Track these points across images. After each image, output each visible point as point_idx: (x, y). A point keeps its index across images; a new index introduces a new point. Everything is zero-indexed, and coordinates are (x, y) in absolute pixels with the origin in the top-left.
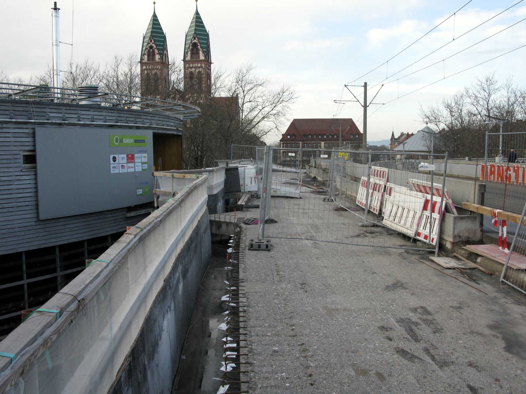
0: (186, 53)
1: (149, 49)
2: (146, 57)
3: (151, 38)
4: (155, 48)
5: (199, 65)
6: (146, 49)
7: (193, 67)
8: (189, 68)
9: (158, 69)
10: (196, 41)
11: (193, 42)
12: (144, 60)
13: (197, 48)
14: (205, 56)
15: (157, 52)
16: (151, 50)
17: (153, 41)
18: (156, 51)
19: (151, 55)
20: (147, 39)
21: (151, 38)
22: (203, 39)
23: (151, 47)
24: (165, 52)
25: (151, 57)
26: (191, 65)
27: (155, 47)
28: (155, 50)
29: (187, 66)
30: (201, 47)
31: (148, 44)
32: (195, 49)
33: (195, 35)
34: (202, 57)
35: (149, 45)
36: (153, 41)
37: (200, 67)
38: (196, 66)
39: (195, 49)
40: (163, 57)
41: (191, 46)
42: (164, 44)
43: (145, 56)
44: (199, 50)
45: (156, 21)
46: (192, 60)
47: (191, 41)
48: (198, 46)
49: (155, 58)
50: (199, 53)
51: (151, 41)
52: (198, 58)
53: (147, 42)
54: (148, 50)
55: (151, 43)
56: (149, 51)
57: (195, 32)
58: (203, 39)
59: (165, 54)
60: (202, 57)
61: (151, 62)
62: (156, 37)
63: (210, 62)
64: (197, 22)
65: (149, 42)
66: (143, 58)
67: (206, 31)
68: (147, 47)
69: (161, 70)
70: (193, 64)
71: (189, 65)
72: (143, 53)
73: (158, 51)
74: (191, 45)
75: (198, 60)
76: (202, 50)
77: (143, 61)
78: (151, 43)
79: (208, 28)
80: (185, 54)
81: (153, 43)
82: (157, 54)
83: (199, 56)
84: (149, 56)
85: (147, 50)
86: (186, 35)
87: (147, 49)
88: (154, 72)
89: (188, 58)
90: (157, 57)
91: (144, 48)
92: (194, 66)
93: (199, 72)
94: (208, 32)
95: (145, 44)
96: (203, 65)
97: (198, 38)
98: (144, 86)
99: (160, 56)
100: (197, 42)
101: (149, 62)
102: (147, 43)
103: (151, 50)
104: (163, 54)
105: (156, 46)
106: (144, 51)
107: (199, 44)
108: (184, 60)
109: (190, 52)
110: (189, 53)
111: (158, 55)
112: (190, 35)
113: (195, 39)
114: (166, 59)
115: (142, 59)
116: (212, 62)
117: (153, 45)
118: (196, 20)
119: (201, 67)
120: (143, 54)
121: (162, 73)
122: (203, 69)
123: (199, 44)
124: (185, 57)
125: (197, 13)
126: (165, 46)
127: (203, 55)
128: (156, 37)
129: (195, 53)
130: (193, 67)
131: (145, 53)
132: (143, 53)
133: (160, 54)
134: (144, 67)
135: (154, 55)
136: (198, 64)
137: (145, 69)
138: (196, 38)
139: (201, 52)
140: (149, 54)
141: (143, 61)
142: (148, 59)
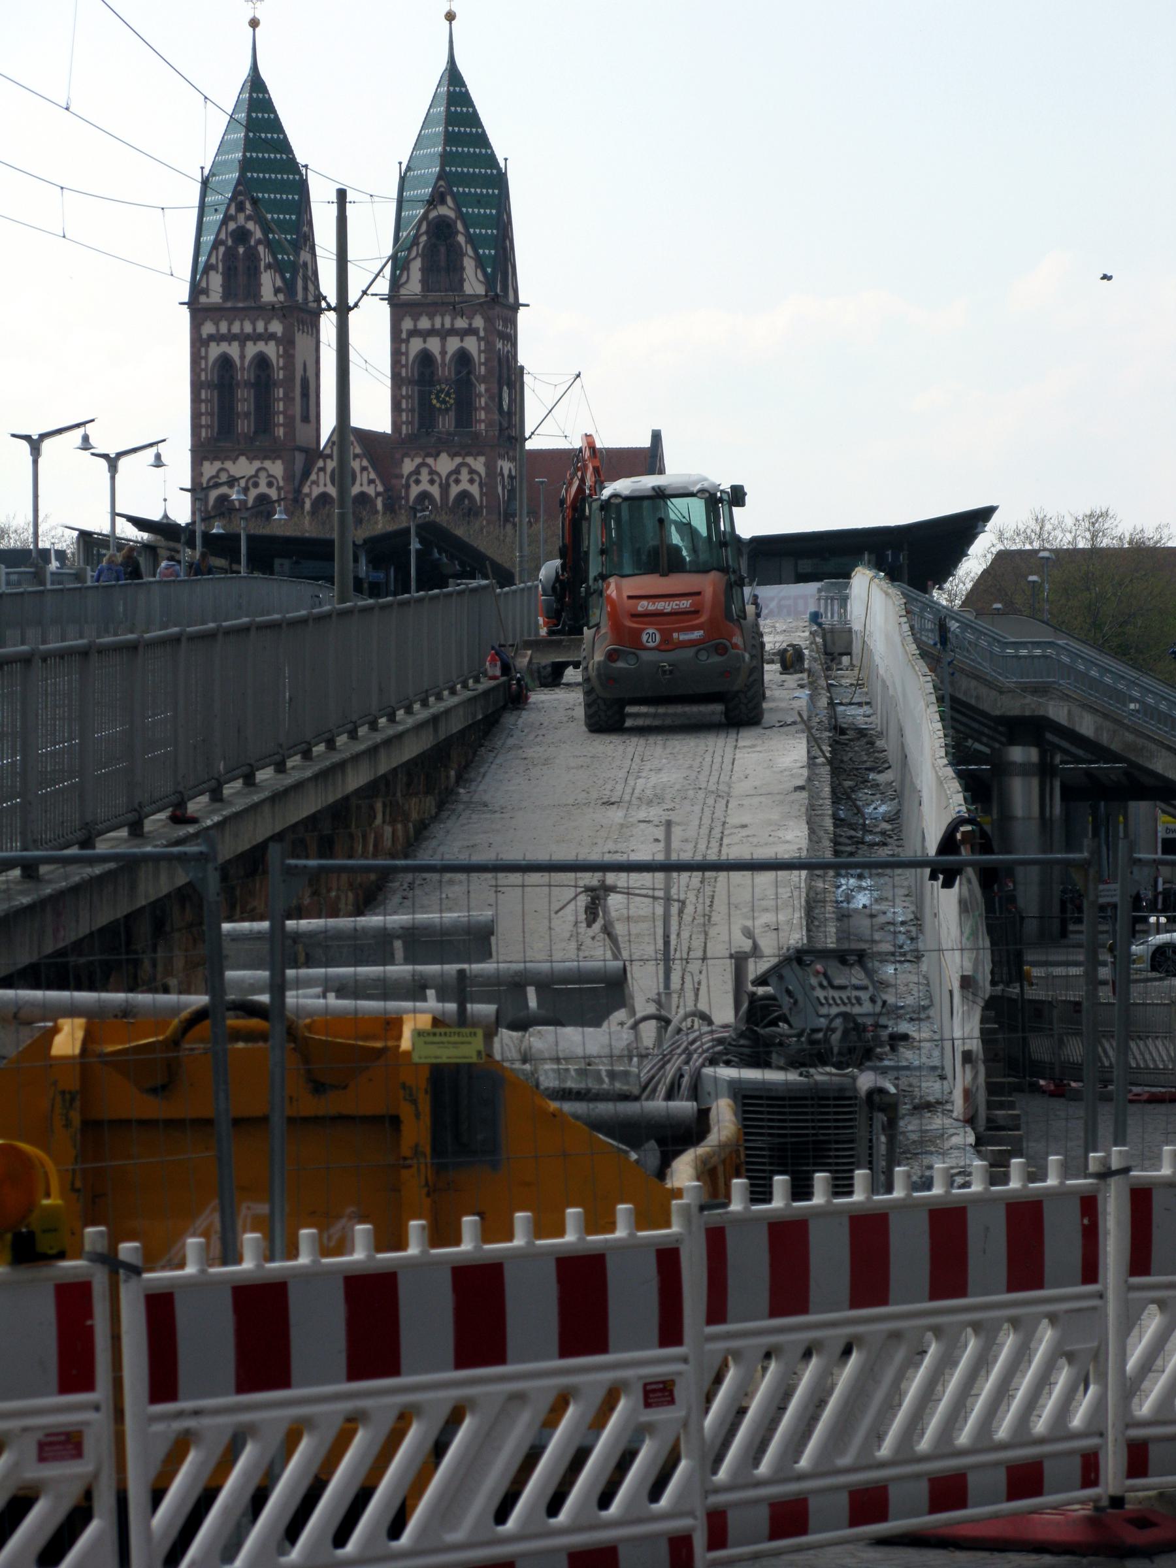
0: (400, 263)
1: (230, 242)
2: (216, 281)
3: (240, 193)
4: (259, 242)
5: (461, 323)
6: (216, 244)
7: (431, 332)
8: (414, 333)
9: (272, 337)
10: (446, 211)
12: (206, 292)
14: (489, 282)
16: (241, 250)
19: (241, 267)
20: (220, 197)
21: (240, 193)
22: (479, 201)
23: (241, 235)
24: (304, 256)
26: (424, 323)
27: (258, 234)
28: (261, 248)
29: (407, 324)
30: (470, 239)
31: (225, 222)
33: (441, 183)
35: (232, 226)
37: (463, 333)
38: (448, 325)
39: (443, 249)
41: (427, 232)
42: (298, 218)
43: (212, 274)
44: (461, 254)
48: (457, 232)
49: (260, 285)
50: (463, 269)
53: (223, 208)
54: (228, 249)
55: (241, 217)
56: (230, 254)
58: (479, 201)
59: (305, 264)
60: (473, 284)
61: (240, 305)
62: (264, 185)
63: (511, 299)
64: (450, 139)
65: (232, 211)
66: (204, 284)
67: (491, 160)
68: (223, 236)
69: (287, 342)
70: (431, 317)
71: (416, 319)
72: (203, 259)
74: (424, 228)
77: (203, 299)
81: (248, 218)
82: (269, 266)
84: (229, 275)
85: (222, 249)
86: (403, 180)
87: (222, 243)
88: (252, 350)
90: (268, 286)
91: (208, 239)
92: (438, 325)
93: (463, 357)
94: (502, 165)
96: (479, 322)
98: (207, 413)
99: (283, 278)
100: (452, 214)
101: (229, 305)
102: (220, 217)
103: (241, 250)
106: (205, 250)
107: (460, 227)
108: (393, 298)
109: (419, 260)
110: (416, 265)
112: (420, 182)
113: (443, 201)
114: (306, 289)
115: (197, 290)
116: (521, 301)
117: (250, 225)
118: (446, 128)
119: (471, 331)
121: (289, 356)
122: (479, 339)
123: (460, 227)
126: (305, 229)
128: (264, 185)
129: (443, 264)
130: (431, 332)
131: (213, 260)
133: (278, 267)
134: (208, 329)
135: (253, 273)
137: (211, 338)
138: (449, 200)
139: (469, 264)
140: (229, 269)
141: (203, 299)
142: (228, 293)
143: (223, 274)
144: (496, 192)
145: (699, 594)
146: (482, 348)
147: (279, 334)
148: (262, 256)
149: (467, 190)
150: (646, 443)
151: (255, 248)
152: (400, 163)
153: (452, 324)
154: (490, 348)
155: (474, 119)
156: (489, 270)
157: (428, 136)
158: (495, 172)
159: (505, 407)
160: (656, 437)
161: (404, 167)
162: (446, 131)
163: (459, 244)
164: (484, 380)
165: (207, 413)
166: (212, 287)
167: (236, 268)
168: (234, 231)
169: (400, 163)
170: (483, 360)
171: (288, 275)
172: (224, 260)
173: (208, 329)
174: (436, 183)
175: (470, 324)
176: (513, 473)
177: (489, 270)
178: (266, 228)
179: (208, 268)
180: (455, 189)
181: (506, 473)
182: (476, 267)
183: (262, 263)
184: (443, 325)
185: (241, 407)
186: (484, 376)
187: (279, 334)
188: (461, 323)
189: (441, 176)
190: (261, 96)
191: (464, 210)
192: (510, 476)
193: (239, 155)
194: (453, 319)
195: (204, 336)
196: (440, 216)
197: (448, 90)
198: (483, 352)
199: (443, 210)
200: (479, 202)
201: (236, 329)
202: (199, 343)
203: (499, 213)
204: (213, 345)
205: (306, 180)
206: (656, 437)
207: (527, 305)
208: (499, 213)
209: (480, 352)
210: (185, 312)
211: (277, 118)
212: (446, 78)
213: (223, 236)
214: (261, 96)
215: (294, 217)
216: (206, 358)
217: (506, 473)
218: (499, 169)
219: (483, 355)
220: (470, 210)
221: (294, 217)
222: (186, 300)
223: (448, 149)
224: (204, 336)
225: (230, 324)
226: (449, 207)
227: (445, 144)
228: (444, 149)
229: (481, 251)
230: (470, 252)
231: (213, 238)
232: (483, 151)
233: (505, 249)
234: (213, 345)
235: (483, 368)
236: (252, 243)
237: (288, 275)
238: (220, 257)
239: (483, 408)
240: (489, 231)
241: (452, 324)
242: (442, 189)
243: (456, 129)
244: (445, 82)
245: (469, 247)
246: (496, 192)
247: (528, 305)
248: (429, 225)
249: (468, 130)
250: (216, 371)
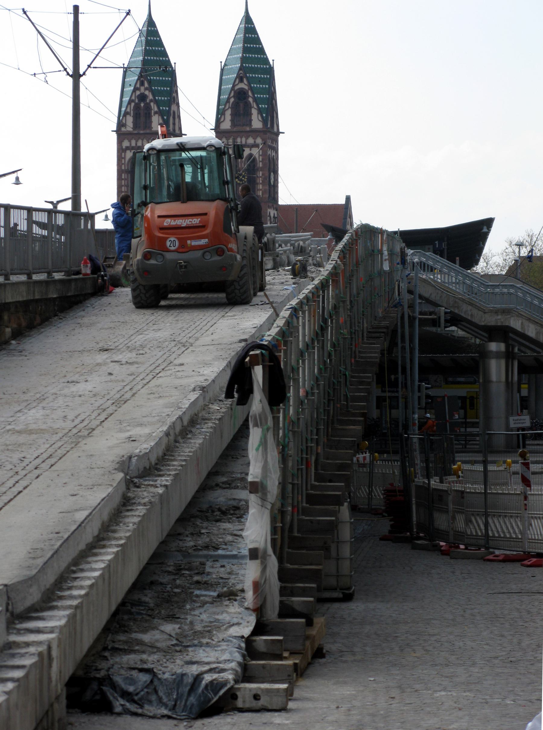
0: (221, 112)
1: (137, 101)
2: (130, 120)
4: (151, 101)
5: (251, 141)
6: (130, 103)
10: (243, 86)
11: (236, 88)
12: (124, 125)
13: (246, 103)
14: (265, 121)
15: (156, 109)
16: (142, 105)
17: (146, 85)
20: (133, 78)
22: (260, 81)
23: (143, 97)
24: (174, 107)
25: (142, 119)
27: (151, 97)
28: (152, 104)
30: (255, 100)
31: (134, 91)
32: (242, 105)
33: (241, 72)
34: (257, 123)
35: (138, 93)
36: (146, 85)
39: (242, 105)
41: (234, 96)
43: (128, 117)
44: (251, 107)
45: (154, 37)
46: (235, 129)
47: (234, 86)
48: (249, 96)
49: (151, 122)
50: (251, 114)
51: (142, 84)
52: (247, 125)
53: (133, 85)
55: (142, 89)
56: (137, 107)
57: (242, 65)
58: (260, 81)
59: (174, 112)
60: (257, 123)
61: (142, 132)
63: (275, 130)
64: (245, 50)
65: (138, 86)
67: (266, 61)
68: (133, 98)
72: (123, 109)
73: (159, 108)
74: (232, 94)
75: (248, 129)
76: (258, 106)
78: (142, 89)
79: (271, 53)
80: (220, 113)
81: (146, 89)
82: (156, 113)
83: (251, 120)
84: (136, 117)
85: (133, 104)
86: (222, 70)
89: (226, 125)
91: (126, 99)
94: (271, 63)
95: (129, 89)
96: (259, 141)
97: (247, 78)
98: (125, 186)
102: (132, 88)
103: (142, 105)
105: (154, 96)
106: (125, 104)
107: (250, 94)
109: (230, 110)
110: (228, 113)
111: (157, 116)
112: (231, 71)
113: (241, 81)
114: (174, 124)
115: (120, 124)
116: (280, 131)
117: (147, 93)
118: (244, 45)
119: (256, 146)
120: (122, 113)
123: (250, 94)
124: (218, 122)
125: (248, 19)
126: (174, 95)
127: (260, 118)
129: (242, 112)
132: (123, 109)
133: (161, 113)
134: (126, 144)
135: (148, 116)
136: (247, 138)
137: (127, 148)
138: (245, 81)
139: (254, 112)
140: (136, 114)
141: (123, 129)
143: (133, 117)
144: (268, 76)
145: (206, 214)
146: (261, 153)
148: (153, 108)
149: (254, 75)
150: (343, 202)
151: (149, 104)
152: (221, 62)
153: (246, 142)
154: (264, 154)
155: (258, 41)
156: (264, 115)
157: (235, 49)
158: (268, 66)
159: (272, 183)
160: (348, 199)
161: (223, 64)
162: (244, 46)
163: (249, 102)
164: (262, 169)
165: (125, 186)
166: (127, 124)
167: (140, 114)
168: (139, 95)
169: (221, 62)
170: (261, 160)
171: (165, 117)
172: (134, 110)
173: (126, 144)
174: (239, 72)
175: (255, 142)
176: (276, 216)
177: (264, 115)
178: (154, 93)
179: (126, 114)
180: (248, 75)
181: (272, 215)
182: (258, 114)
183: (153, 111)
184: (241, 142)
186: (262, 167)
188: (251, 141)
189: (240, 69)
190: (153, 29)
191: (252, 85)
192: (274, 217)
193: (141, 58)
194: (246, 139)
195: (124, 147)
196: (239, 89)
197: (245, 26)
198: (261, 155)
199: (241, 86)
200: (260, 81)
202: (121, 151)
203: (270, 87)
204: (128, 152)
205: (175, 70)
206: (348, 199)
207: (283, 133)
208: (270, 87)
209: (259, 155)
210: (115, 135)
211: (160, 40)
212: (244, 20)
213: (133, 98)
214: (153, 29)
215: (168, 89)
216: (125, 158)
217: (272, 215)
218: (270, 65)
219: (261, 157)
220: (255, 85)
221: (168, 89)
222: (115, 129)
223: (245, 55)
224: (124, 147)
225: (137, 142)
226: (245, 84)
227: (243, 53)
228: (243, 55)
229: (260, 106)
230: (255, 106)
231: (128, 98)
232: (262, 56)
233: (272, 104)
234: (128, 152)
235: (261, 163)
236: (148, 101)
237: (165, 117)
238: (132, 108)
239: (261, 184)
240: (265, 96)
241: (246, 142)
242: (241, 75)
243: (249, 45)
244: (244, 22)
245: (254, 104)
246: (268, 76)
247: (283, 133)
248: (235, 92)
249: (255, 46)
250: (130, 165)
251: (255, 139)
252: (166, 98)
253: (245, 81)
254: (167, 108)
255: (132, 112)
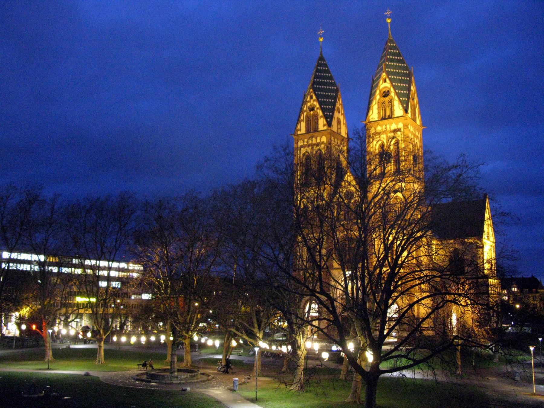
4: (318, 109)
12: (300, 130)
18: (320, 113)
27: (318, 106)
30: (397, 94)
36: (314, 97)
40: (331, 120)
51: (311, 97)
55: (312, 101)
66: (299, 127)
73: (323, 112)
81: (314, 101)
82: (321, 117)
97: (390, 79)
99: (327, 121)
104: (331, 117)
107: (392, 90)
111: (322, 119)
133: (326, 117)
137: (302, 147)
138: (387, 80)
147: (325, 142)
166: (302, 128)
178: (320, 103)
183: (319, 116)
185: (367, 220)
187: (325, 142)
201: (310, 142)
204: (302, 149)
251: (397, 124)
252: (330, 107)
253: (387, 80)
254: (331, 114)
255: (305, 119)
